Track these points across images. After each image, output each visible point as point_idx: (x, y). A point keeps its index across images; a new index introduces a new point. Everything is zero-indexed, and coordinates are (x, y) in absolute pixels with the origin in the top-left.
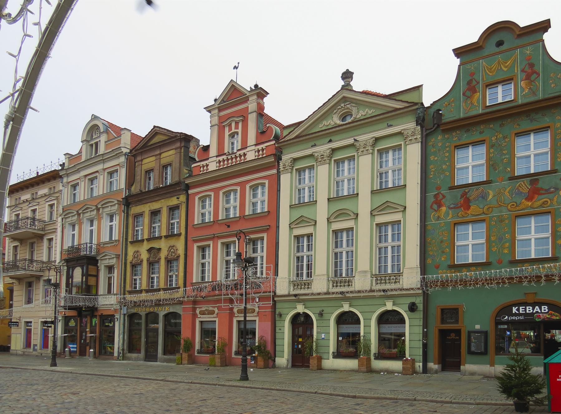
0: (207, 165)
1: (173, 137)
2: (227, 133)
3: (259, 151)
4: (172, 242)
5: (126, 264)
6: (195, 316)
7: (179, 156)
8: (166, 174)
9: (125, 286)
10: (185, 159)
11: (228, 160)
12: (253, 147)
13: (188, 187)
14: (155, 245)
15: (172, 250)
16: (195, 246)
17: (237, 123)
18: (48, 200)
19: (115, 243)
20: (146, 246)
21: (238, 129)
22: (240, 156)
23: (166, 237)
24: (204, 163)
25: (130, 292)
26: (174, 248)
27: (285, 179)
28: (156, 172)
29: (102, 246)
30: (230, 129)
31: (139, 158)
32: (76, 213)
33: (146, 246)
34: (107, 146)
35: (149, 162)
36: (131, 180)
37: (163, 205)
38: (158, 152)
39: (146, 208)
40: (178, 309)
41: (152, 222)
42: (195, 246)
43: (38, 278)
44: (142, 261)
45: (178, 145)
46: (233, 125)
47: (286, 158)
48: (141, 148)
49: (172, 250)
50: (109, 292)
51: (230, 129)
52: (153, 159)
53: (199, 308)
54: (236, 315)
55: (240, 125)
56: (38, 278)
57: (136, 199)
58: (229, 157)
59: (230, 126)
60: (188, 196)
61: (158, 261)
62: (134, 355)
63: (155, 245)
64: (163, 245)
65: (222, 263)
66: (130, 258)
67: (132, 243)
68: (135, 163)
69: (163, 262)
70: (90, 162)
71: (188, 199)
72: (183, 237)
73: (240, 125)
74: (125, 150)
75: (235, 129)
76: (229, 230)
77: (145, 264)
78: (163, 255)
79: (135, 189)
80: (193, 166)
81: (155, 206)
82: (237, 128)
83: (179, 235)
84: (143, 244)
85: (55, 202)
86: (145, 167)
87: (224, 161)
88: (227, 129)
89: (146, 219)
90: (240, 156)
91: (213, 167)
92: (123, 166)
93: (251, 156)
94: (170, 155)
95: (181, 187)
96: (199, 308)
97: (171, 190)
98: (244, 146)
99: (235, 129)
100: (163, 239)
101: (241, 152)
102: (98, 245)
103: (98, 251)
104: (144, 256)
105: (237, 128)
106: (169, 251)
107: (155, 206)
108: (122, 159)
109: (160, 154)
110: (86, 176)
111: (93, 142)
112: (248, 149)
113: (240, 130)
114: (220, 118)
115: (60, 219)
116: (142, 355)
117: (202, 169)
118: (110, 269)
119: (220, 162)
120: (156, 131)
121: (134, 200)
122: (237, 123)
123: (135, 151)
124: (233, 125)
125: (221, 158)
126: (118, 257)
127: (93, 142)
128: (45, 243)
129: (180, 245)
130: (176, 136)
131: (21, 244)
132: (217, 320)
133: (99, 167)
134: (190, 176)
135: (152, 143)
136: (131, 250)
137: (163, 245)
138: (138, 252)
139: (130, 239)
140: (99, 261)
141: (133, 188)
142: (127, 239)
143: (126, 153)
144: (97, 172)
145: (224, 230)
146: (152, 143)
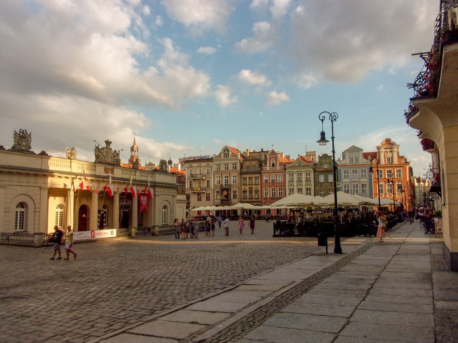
4: (257, 186)
14: (252, 186)
25: (243, 199)
27: (287, 176)
35: (247, 163)
36: (242, 167)
37: (253, 176)
39: (247, 176)
47: (287, 171)
61: (252, 191)
63: (252, 186)
64: (254, 187)
66: (242, 189)
72: (260, 185)
78: (254, 189)
81: (250, 176)
89: (248, 179)
94: (254, 163)
104: (248, 189)
115: (212, 175)
128: (206, 181)
129: (259, 188)
136: (243, 187)
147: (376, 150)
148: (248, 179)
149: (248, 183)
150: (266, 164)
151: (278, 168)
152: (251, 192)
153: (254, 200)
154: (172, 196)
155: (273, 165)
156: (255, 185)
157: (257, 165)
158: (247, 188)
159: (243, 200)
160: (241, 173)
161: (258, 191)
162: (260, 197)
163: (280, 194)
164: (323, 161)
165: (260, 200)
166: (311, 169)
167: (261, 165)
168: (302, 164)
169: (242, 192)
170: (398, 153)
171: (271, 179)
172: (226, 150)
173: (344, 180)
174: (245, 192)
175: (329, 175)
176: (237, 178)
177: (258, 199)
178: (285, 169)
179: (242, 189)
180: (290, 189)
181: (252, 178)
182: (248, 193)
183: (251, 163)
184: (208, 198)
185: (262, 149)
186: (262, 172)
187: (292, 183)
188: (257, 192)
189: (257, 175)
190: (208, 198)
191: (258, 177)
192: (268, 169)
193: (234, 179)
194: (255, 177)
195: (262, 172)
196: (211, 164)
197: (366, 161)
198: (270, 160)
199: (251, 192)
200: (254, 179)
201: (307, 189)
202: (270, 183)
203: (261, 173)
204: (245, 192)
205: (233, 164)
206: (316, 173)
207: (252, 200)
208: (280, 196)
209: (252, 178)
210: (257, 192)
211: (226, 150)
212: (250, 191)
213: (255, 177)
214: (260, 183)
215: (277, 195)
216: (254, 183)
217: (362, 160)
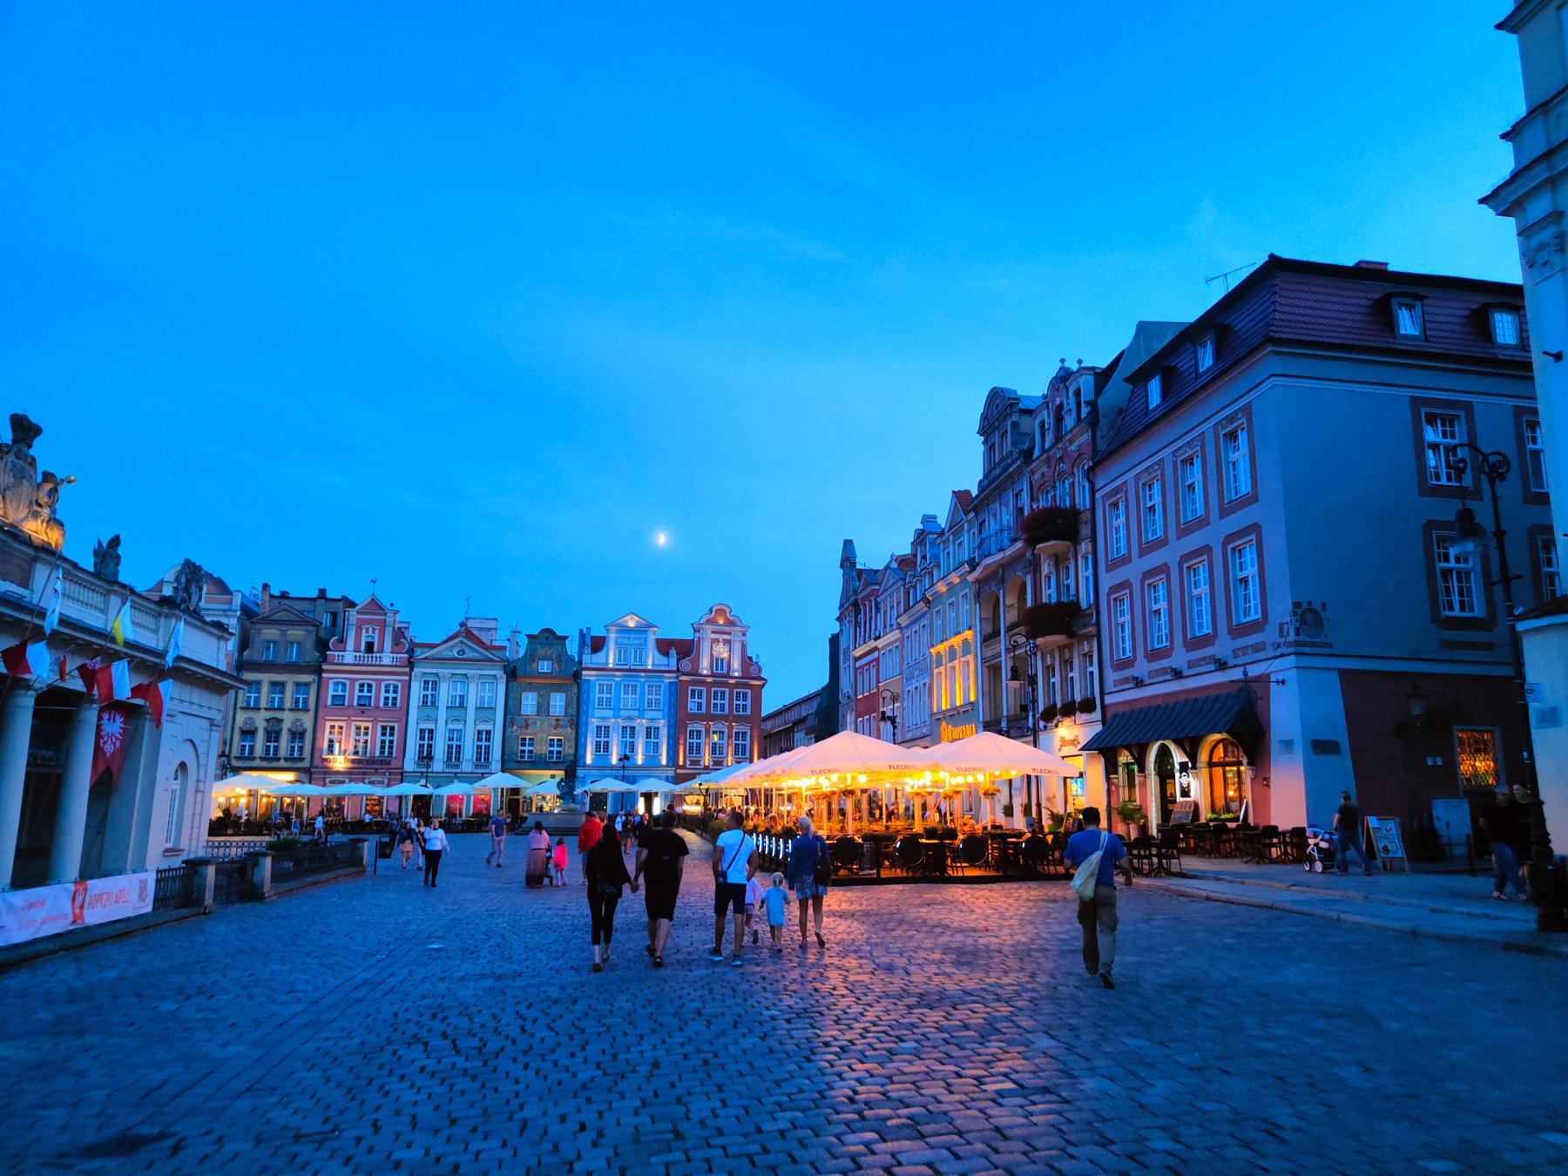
4: (300, 715)
14: (278, 715)
20: (264, 715)
25: (237, 758)
33: (264, 715)
37: (289, 679)
39: (266, 678)
61: (278, 733)
63: (278, 715)
64: (288, 718)
72: (311, 714)
78: (286, 726)
89: (265, 689)
94: (296, 633)
106: (293, 723)
129: (307, 720)
136: (241, 717)
147: (688, 635)
148: (265, 689)
149: (263, 704)
150: (342, 641)
151: (387, 658)
152: (273, 735)
154: (206, 724)
155: (370, 647)
156: (295, 709)
157: (310, 643)
158: (260, 719)
159: (235, 763)
163: (383, 747)
164: (542, 651)
165: (306, 764)
166: (500, 673)
167: (322, 645)
168: (469, 654)
169: (237, 732)
170: (744, 647)
171: (357, 693)
173: (598, 713)
174: (249, 733)
175: (553, 695)
177: (301, 759)
178: (411, 665)
180: (480, 732)
181: (283, 684)
182: (261, 736)
183: (284, 633)
185: (322, 592)
186: (325, 667)
187: (428, 711)
188: (297, 735)
191: (307, 684)
192: (349, 657)
194: (298, 684)
195: (325, 667)
197: (664, 660)
198: (359, 629)
199: (273, 735)
200: (289, 688)
201: (480, 732)
202: (377, 707)
203: (319, 671)
204: (249, 733)
206: (514, 684)
207: (274, 764)
208: (382, 752)
209: (283, 684)
210: (297, 735)
214: (312, 705)
215: (373, 750)
216: (288, 704)
217: (652, 659)
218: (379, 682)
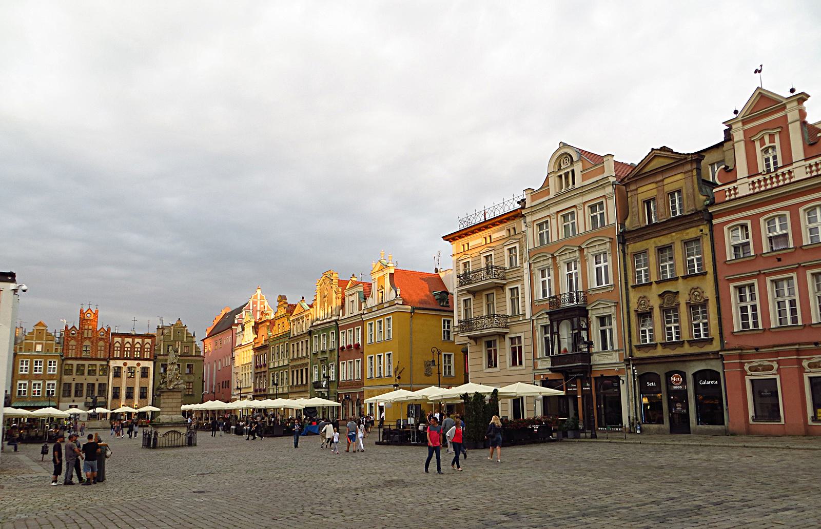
0: (735, 189)
1: (681, 160)
2: (758, 149)
3: (810, 166)
4: (695, 283)
5: (628, 312)
6: (744, 373)
7: (691, 180)
8: (673, 202)
9: (630, 341)
10: (699, 184)
11: (765, 180)
12: (803, 163)
13: (711, 216)
15: (696, 293)
16: (732, 286)
17: (772, 136)
18: (507, 243)
19: (609, 289)
20: (656, 290)
21: (775, 142)
22: (783, 174)
23: (684, 277)
24: (731, 186)
25: (639, 347)
26: (699, 290)
28: (661, 202)
29: (591, 293)
30: (762, 144)
31: (633, 187)
32: (547, 254)
33: (656, 290)
34: (584, 178)
35: (647, 190)
37: (675, 239)
38: (659, 178)
39: (651, 245)
40: (715, 365)
41: (660, 261)
42: (732, 286)
43: (502, 335)
44: (652, 309)
45: (688, 167)
46: (767, 139)
48: (634, 177)
49: (696, 293)
50: (605, 347)
51: (762, 144)
52: (653, 186)
53: (748, 362)
54: (807, 371)
55: (777, 138)
56: (502, 335)
57: (635, 235)
58: (767, 177)
59: (762, 140)
60: (711, 225)
61: (676, 309)
62: (654, 426)
64: (682, 287)
65: (737, 308)
66: (634, 305)
67: (633, 287)
68: (627, 192)
69: (683, 309)
70: (560, 197)
71: (711, 231)
72: (710, 276)
73: (777, 138)
74: (612, 179)
75: (770, 142)
76: (780, 263)
77: (657, 313)
78: (683, 300)
79: (631, 223)
80: (714, 191)
81: (664, 241)
82: (772, 139)
83: (705, 274)
84: (650, 289)
85: (517, 245)
86: (642, 197)
87: (759, 181)
88: (758, 144)
89: (652, 259)
90: (783, 174)
91: (744, 189)
92: (611, 198)
93: (800, 173)
94: (675, 180)
95: (704, 216)
96: (748, 362)
97: (687, 221)
98: (788, 162)
99: (770, 142)
100: (680, 280)
101: (785, 170)
102: (585, 292)
103: (586, 301)
104: (655, 302)
105: (772, 139)
107: (664, 241)
108: (609, 190)
109: (663, 180)
110: (558, 212)
111: (562, 173)
112: (794, 165)
113: (777, 144)
114: (744, 131)
115: (526, 265)
116: (666, 425)
117: (727, 193)
118: (602, 320)
119: (753, 183)
120: (655, 154)
121: (633, 236)
122: (772, 136)
123: (628, 179)
124: (767, 139)
125: (755, 179)
126: (617, 305)
127: (562, 173)
130: (686, 158)
131: (474, 296)
132: (778, 377)
133: (577, 201)
134: (712, 204)
135: (646, 170)
136: (634, 297)
137: (682, 287)
138: (645, 297)
139: (631, 284)
140: (590, 312)
141: (627, 223)
142: (626, 283)
143: (613, 182)
144: (575, 206)
145: (773, 265)
146: (646, 170)
152: (669, 310)
153: (687, 349)
160: (625, 238)
161: (704, 304)
162: (714, 332)
165: (715, 346)
171: (765, 234)
172: (565, 157)
176: (609, 263)
179: (634, 305)
184: (516, 359)
188: (697, 307)
189: (692, 233)
190: (516, 359)
191: (697, 240)
193: (597, 271)
194: (686, 243)
196: (520, 225)
205: (593, 208)
207: (678, 351)
209: (670, 247)
211: (565, 157)
212: (665, 311)
213: (686, 243)
214: (709, 268)
218: (794, 209)
